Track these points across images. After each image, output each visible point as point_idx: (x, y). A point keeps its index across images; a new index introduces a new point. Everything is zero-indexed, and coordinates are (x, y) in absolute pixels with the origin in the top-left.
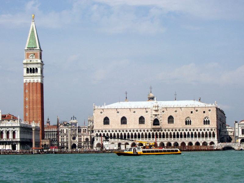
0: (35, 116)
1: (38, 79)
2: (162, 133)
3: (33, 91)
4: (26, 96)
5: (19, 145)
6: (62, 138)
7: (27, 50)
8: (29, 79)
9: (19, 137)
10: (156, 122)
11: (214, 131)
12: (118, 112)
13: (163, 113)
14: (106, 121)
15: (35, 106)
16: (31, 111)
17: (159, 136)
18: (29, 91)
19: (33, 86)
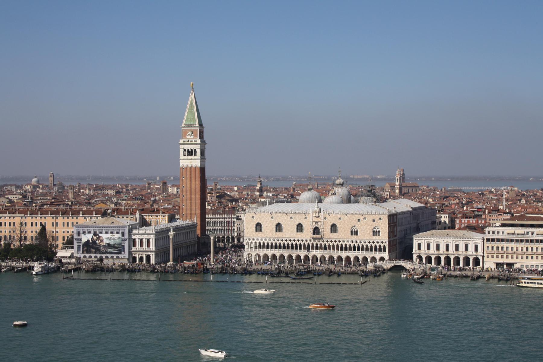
0: (193, 207)
2: (323, 244)
3: (191, 177)
5: (154, 256)
10: (316, 231)
11: (386, 245)
12: (272, 217)
14: (258, 227)
15: (193, 196)
16: (189, 202)
18: (186, 177)
19: (191, 171)
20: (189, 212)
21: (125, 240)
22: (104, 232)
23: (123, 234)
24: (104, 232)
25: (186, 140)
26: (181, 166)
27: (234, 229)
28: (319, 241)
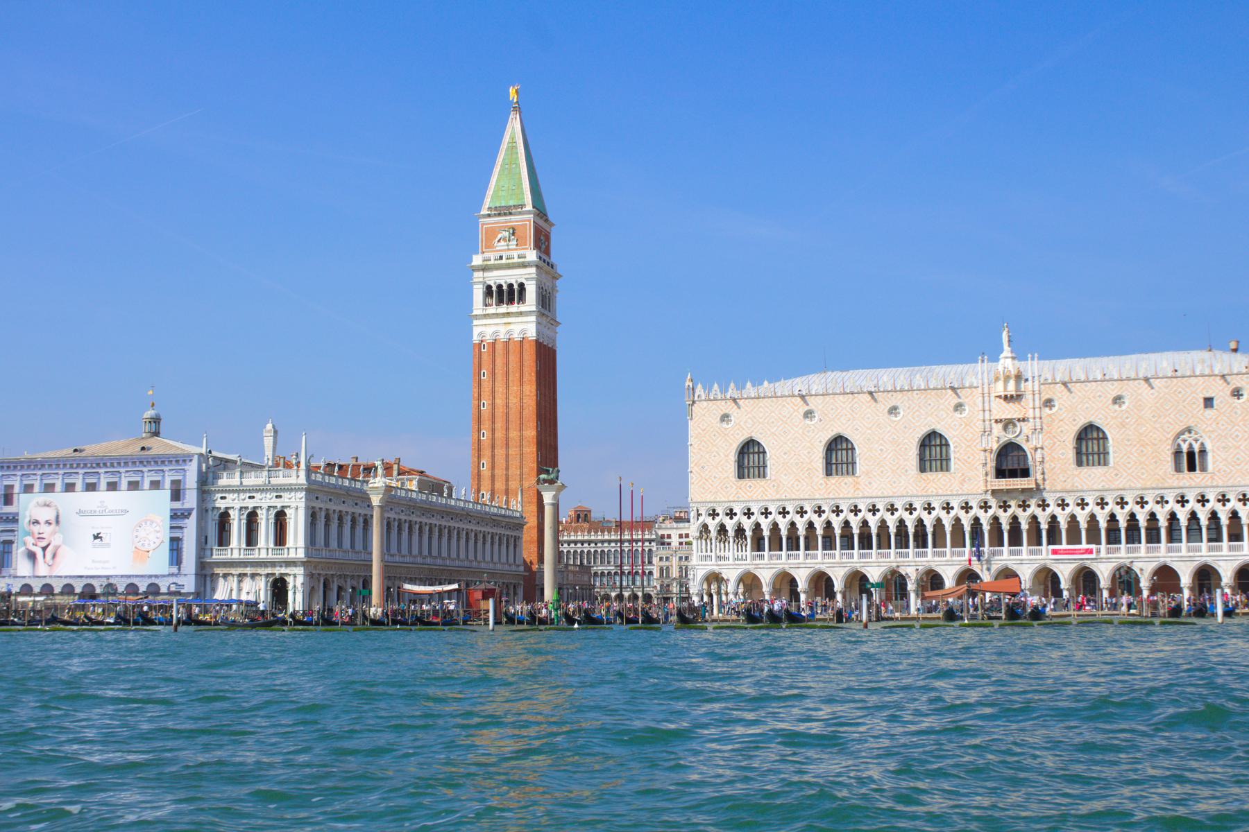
0: (514, 471)
1: (525, 326)
3: (507, 373)
4: (479, 395)
6: (664, 563)
7: (489, 216)
8: (493, 329)
9: (301, 543)
10: (1010, 462)
13: (1047, 410)
14: (750, 458)
15: (514, 434)
16: (500, 452)
17: (1028, 531)
18: (493, 373)
20: (499, 485)
21: (185, 514)
22: (103, 485)
23: (176, 495)
24: (103, 485)
25: (492, 256)
26: (476, 339)
27: (651, 573)
28: (1024, 506)
